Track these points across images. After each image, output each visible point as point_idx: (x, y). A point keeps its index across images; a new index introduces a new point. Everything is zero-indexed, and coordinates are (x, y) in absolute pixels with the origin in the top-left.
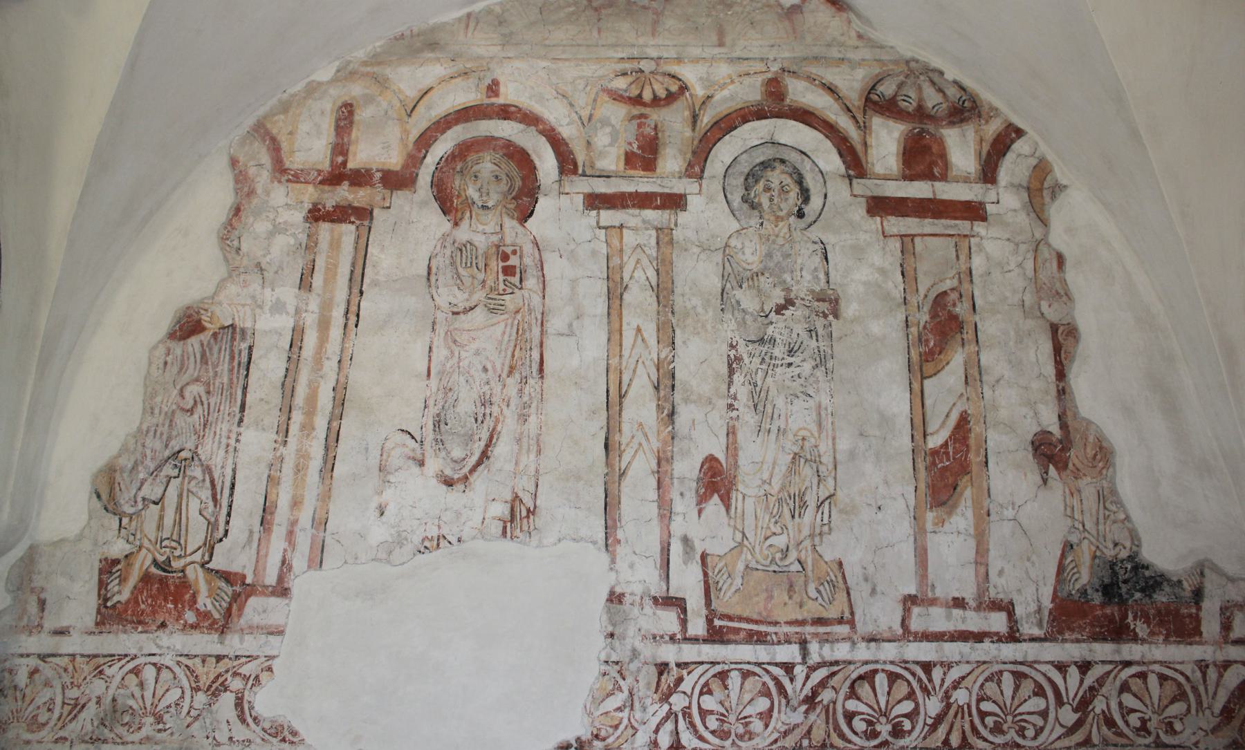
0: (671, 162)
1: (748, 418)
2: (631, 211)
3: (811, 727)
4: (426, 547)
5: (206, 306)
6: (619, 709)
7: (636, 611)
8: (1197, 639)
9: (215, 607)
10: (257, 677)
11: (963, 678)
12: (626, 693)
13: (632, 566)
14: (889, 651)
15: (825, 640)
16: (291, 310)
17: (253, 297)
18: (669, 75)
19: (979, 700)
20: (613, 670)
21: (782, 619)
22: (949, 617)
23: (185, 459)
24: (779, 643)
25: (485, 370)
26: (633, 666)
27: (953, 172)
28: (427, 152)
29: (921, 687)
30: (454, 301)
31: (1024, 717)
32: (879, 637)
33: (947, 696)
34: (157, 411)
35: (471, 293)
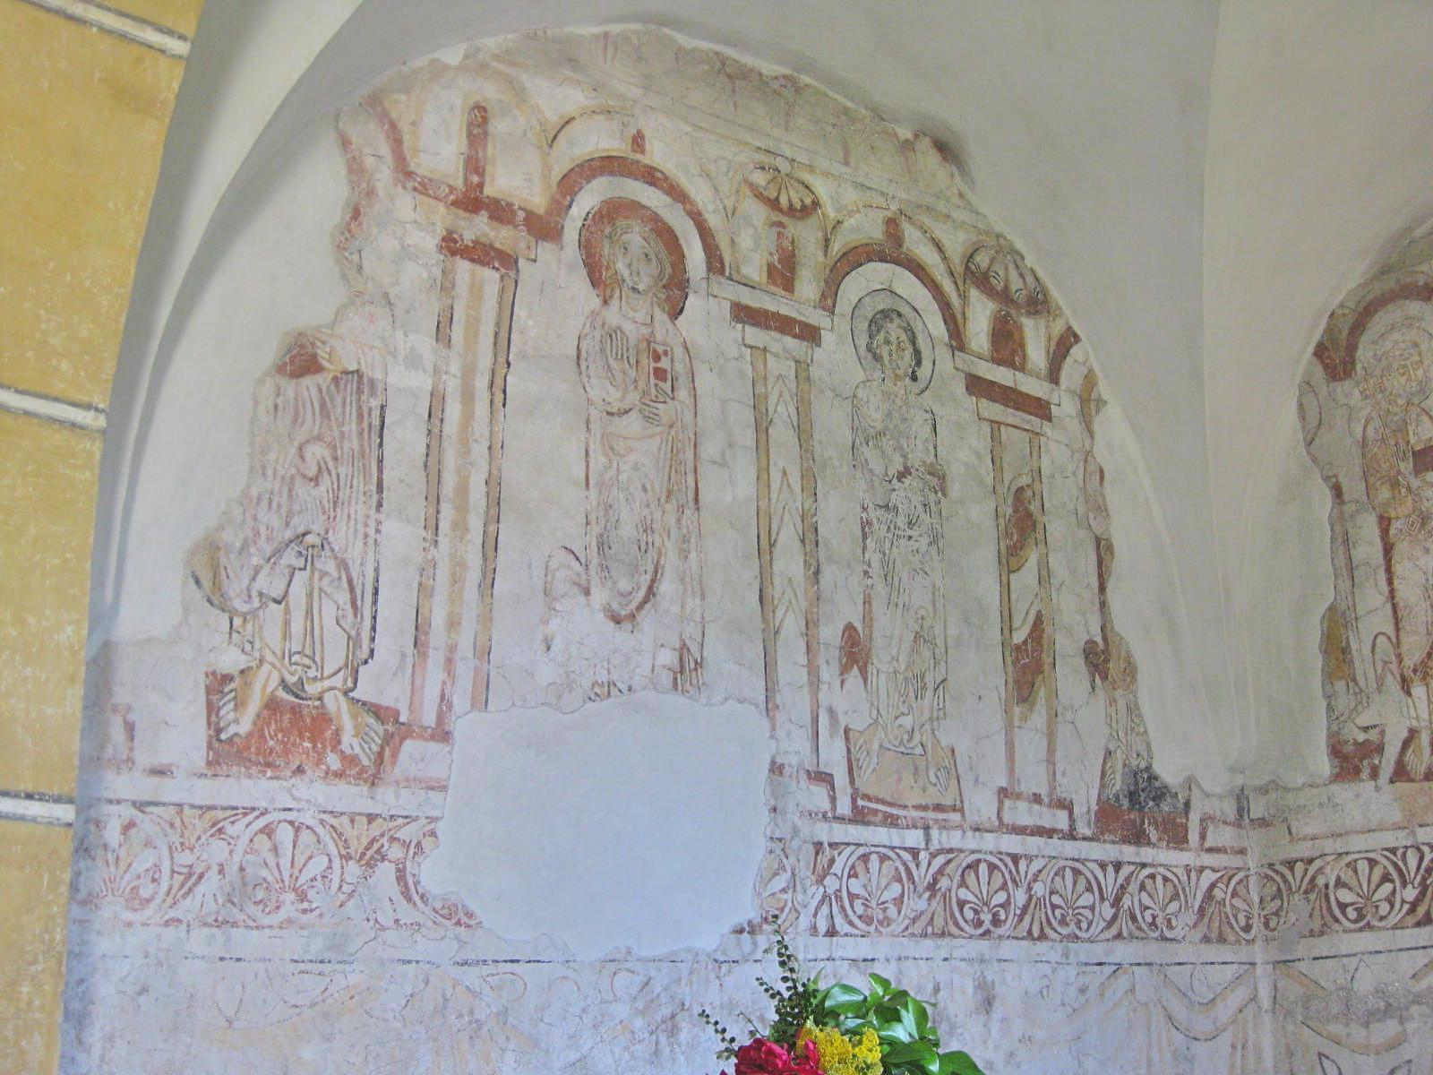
0: (808, 287)
1: (881, 589)
2: (773, 333)
3: (933, 914)
4: (597, 694)
5: (324, 338)
6: (784, 891)
8: (1185, 845)
9: (363, 748)
10: (419, 844)
11: (1040, 871)
12: (789, 873)
13: (789, 734)
14: (989, 842)
15: (945, 826)
16: (429, 367)
17: (383, 339)
18: (803, 183)
20: (778, 847)
21: (910, 803)
23: (313, 546)
24: (908, 827)
25: (644, 489)
26: (795, 844)
27: (1029, 366)
28: (572, 201)
30: (608, 399)
31: (1080, 910)
33: (1030, 889)
34: (270, 472)
35: (625, 392)
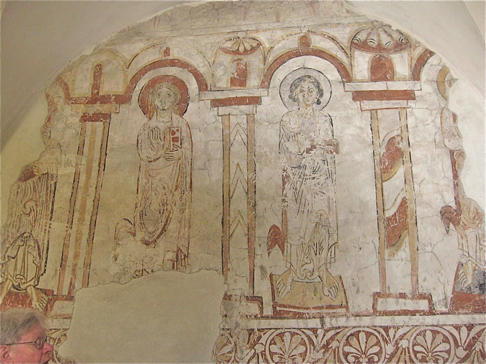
0: (253, 81)
1: (293, 206)
2: (233, 107)
4: (137, 275)
5: (35, 165)
6: (230, 352)
7: (238, 303)
9: (40, 306)
10: (59, 339)
11: (405, 334)
12: (233, 344)
13: (235, 281)
14: (366, 321)
15: (333, 316)
16: (74, 165)
17: (57, 159)
18: (252, 38)
19: (413, 346)
20: (226, 333)
22: (397, 303)
23: (27, 237)
24: (310, 318)
25: (164, 188)
28: (136, 85)
29: (383, 339)
30: (149, 156)
31: (438, 353)
32: (361, 314)
33: (397, 343)
34: (14, 215)
35: (157, 151)
